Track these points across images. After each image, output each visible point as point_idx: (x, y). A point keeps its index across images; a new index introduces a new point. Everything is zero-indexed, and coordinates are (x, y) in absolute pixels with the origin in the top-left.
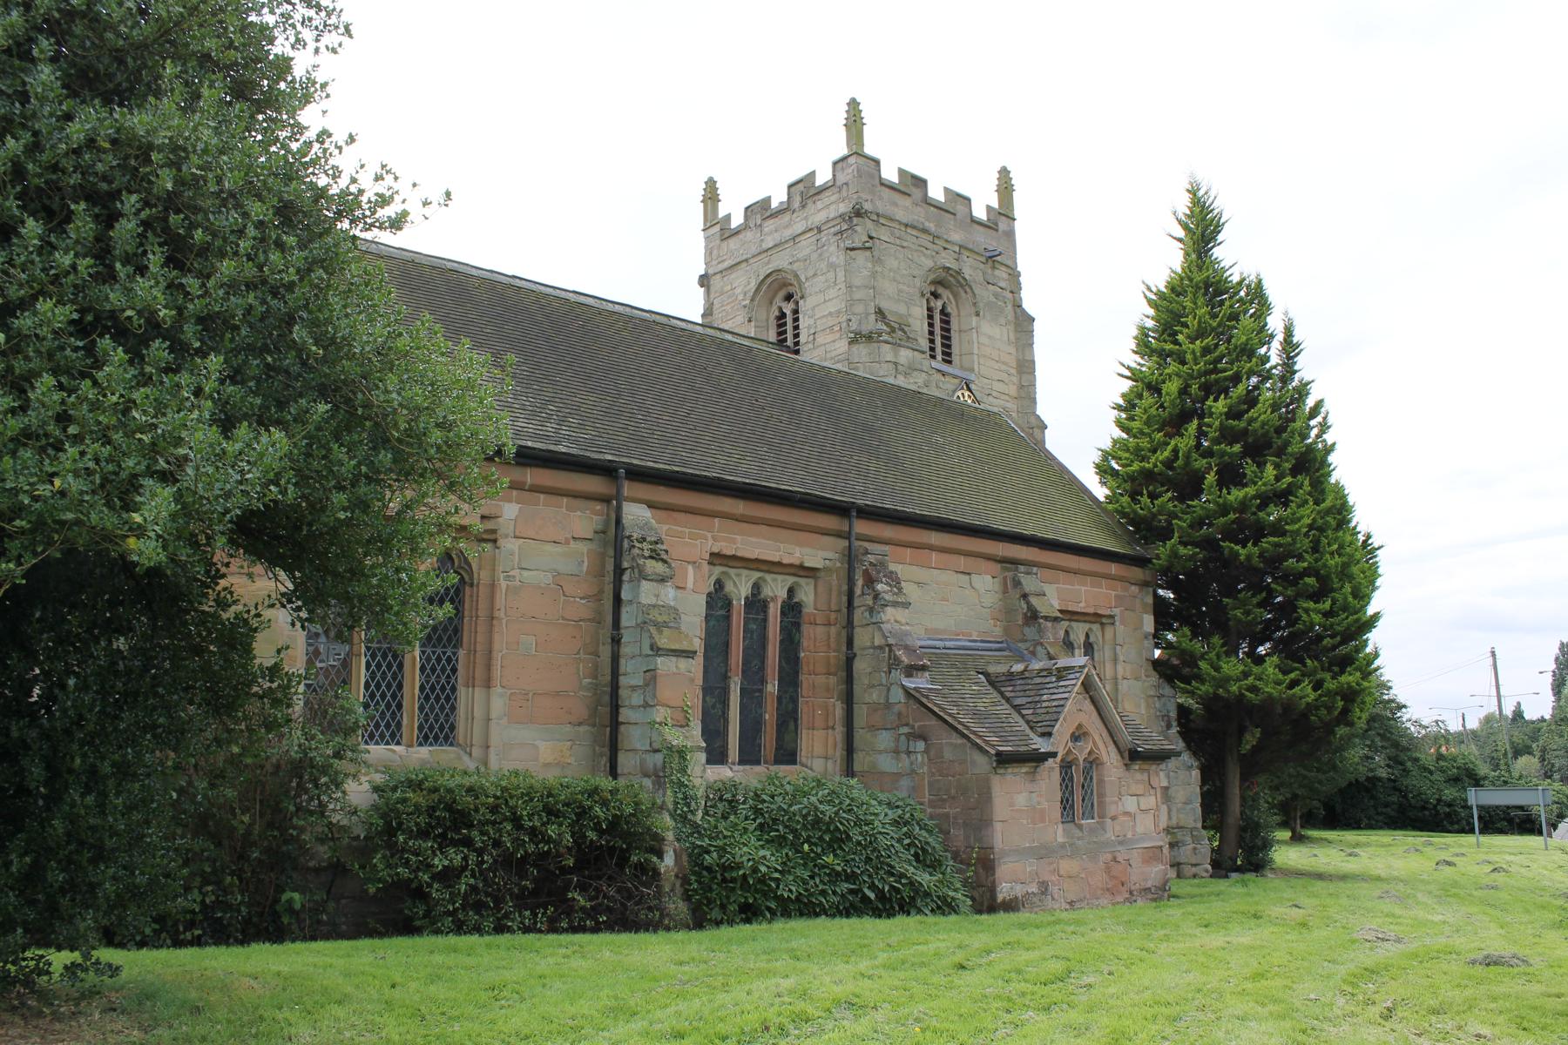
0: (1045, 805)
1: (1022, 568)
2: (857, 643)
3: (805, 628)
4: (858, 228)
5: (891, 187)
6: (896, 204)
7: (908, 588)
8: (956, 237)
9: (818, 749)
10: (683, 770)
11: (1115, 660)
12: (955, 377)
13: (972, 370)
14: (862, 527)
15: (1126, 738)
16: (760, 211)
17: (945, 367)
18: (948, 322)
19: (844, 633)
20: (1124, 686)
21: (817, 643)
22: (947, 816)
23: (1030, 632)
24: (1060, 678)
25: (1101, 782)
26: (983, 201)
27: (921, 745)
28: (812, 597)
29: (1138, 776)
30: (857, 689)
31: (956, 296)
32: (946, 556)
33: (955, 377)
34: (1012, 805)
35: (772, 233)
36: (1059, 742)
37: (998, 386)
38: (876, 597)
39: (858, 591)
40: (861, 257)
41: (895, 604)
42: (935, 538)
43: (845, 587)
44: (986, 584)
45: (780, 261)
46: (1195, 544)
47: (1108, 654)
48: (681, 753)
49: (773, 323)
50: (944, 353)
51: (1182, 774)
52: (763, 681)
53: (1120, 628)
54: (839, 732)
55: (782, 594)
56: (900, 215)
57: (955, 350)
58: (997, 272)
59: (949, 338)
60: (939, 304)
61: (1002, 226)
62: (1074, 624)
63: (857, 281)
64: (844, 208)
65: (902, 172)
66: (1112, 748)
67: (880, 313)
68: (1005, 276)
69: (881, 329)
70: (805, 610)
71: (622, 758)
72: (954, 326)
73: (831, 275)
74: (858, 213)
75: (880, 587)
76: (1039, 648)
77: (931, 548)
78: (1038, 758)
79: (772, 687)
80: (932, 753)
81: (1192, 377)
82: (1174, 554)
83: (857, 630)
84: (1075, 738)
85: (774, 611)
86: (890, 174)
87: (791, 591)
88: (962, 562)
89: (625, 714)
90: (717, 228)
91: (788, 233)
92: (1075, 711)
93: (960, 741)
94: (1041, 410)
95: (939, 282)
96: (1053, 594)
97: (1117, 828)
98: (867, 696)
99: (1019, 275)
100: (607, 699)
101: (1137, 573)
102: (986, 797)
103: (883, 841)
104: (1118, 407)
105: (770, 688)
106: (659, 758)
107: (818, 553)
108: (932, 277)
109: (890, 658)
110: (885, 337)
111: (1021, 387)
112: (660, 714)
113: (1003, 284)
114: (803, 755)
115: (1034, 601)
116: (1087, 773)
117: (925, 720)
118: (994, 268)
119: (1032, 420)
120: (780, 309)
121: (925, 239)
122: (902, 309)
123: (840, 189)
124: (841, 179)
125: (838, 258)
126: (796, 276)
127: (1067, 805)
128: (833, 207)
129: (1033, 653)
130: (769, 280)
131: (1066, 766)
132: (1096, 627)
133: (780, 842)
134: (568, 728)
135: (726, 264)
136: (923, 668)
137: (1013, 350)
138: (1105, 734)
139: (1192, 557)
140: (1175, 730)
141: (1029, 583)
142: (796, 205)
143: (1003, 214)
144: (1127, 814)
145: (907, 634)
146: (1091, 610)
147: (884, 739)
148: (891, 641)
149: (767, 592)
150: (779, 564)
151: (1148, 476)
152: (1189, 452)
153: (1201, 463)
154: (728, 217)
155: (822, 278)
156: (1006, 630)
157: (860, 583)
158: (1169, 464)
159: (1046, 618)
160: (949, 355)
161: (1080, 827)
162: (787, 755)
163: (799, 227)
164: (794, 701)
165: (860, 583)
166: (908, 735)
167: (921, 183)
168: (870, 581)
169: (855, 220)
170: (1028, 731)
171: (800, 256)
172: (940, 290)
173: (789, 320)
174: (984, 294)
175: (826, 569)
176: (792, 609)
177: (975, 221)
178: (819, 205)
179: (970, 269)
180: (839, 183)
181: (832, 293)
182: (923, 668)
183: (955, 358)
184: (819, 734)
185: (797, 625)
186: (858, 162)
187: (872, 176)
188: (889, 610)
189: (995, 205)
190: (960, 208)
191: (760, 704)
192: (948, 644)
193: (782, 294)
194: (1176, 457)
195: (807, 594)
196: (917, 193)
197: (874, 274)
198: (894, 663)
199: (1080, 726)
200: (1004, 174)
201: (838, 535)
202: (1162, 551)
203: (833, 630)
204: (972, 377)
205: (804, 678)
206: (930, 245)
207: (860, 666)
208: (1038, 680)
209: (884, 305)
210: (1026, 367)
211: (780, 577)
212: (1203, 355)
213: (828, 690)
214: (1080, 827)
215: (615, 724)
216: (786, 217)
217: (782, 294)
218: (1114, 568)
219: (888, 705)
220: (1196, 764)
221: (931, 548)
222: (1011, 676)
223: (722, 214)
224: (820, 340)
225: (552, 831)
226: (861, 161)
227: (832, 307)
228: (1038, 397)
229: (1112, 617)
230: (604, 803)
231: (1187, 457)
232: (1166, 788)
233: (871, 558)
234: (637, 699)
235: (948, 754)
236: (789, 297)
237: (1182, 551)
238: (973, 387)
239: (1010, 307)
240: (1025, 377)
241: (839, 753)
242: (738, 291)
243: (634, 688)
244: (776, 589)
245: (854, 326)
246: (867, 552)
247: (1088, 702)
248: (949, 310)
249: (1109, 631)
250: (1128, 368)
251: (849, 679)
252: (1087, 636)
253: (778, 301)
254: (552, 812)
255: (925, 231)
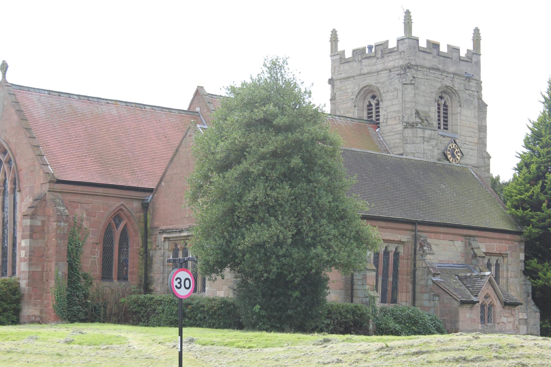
0: (475, 317)
1: (472, 238)
2: (417, 265)
3: (400, 260)
4: (409, 74)
5: (424, 51)
6: (425, 59)
7: (433, 247)
8: (452, 69)
9: (404, 300)
10: (374, 303)
11: (507, 270)
12: (449, 137)
13: (457, 133)
14: (419, 228)
15: (503, 298)
16: (358, 53)
17: (444, 133)
18: (446, 110)
19: (413, 262)
20: (511, 280)
21: (404, 265)
22: (445, 320)
23: (474, 261)
24: (481, 279)
25: (494, 312)
26: (465, 46)
27: (437, 298)
28: (402, 250)
29: (507, 311)
30: (417, 280)
31: (451, 97)
32: (445, 235)
33: (449, 137)
34: (465, 316)
35: (367, 66)
36: (480, 298)
37: (469, 139)
38: (424, 251)
39: (418, 249)
40: (410, 88)
41: (430, 254)
42: (442, 230)
43: (413, 248)
44: (459, 244)
45: (370, 81)
46: (540, 228)
47: (505, 268)
48: (374, 298)
49: (365, 108)
50: (444, 125)
51: (533, 314)
52: (387, 277)
53: (510, 258)
54: (410, 294)
55: (394, 250)
56: (428, 64)
57: (450, 123)
58: (471, 84)
59: (447, 117)
60: (443, 102)
61: (474, 59)
62: (492, 257)
63: (407, 99)
64: (401, 62)
65: (428, 42)
66: (498, 301)
67: (417, 113)
68: (474, 85)
69: (419, 121)
70: (400, 254)
71: (354, 299)
72: (449, 111)
73: (395, 93)
74: (409, 67)
75: (425, 248)
76: (477, 267)
77: (441, 233)
78: (473, 303)
79: (391, 279)
80: (441, 301)
81: (542, 163)
82: (530, 232)
83: (417, 262)
84: (487, 297)
85: (391, 255)
86: (423, 44)
87: (396, 248)
88: (451, 237)
89: (355, 287)
90: (338, 57)
91: (374, 68)
92: (486, 289)
93: (450, 297)
94: (488, 150)
95: (444, 92)
96: (482, 247)
97: (499, 327)
98: (420, 282)
99: (481, 82)
100: (349, 282)
101: (518, 237)
102: (457, 314)
103: (428, 324)
104: (515, 169)
105: (390, 279)
106: (367, 299)
107: (405, 237)
108: (440, 91)
109: (428, 270)
110: (419, 126)
111: (480, 138)
112: (367, 287)
113: (473, 89)
114: (399, 301)
115: (476, 251)
116: (489, 309)
117: (438, 290)
118: (469, 81)
119: (484, 154)
120: (370, 102)
121: (438, 74)
122: (426, 109)
123: (401, 53)
124: (401, 48)
125: (399, 86)
126: (379, 90)
127: (482, 318)
128: (397, 61)
129: (475, 269)
130: (365, 89)
131: (483, 306)
132: (500, 258)
133: (400, 323)
134: (338, 291)
135: (343, 76)
136: (438, 274)
137: (476, 121)
138: (496, 297)
139: (537, 233)
140: (530, 297)
141: (474, 244)
142: (379, 55)
143: (475, 52)
144: (503, 323)
145: (433, 263)
146: (498, 252)
147: (426, 296)
148: (428, 265)
149: (389, 249)
150: (394, 241)
151: (523, 200)
152: (538, 194)
153: (542, 197)
154: (343, 52)
155: (391, 94)
156: (466, 260)
157: (418, 246)
158: (531, 197)
159: (479, 257)
160: (447, 125)
161: (487, 325)
162: (394, 301)
163: (380, 67)
164: (396, 283)
165: (418, 246)
166: (434, 295)
167: (436, 46)
168: (422, 246)
169: (407, 70)
170: (471, 295)
171: (381, 81)
172: (444, 95)
173: (374, 107)
174: (464, 95)
175: (408, 241)
176: (396, 254)
177: (460, 59)
178: (390, 58)
179: (458, 85)
180: (400, 50)
181: (396, 102)
182: (438, 274)
183: (449, 127)
184: (404, 294)
185: (398, 259)
186: (409, 40)
187: (415, 48)
188: (428, 256)
189: (471, 48)
190: (455, 55)
191: (386, 285)
192: (446, 265)
193: (370, 95)
194: (533, 195)
195: (401, 250)
196: (435, 52)
197: (415, 94)
198: (429, 273)
199: (487, 294)
200: (477, 31)
201: (412, 231)
202: (527, 230)
203: (409, 261)
204: (457, 136)
205: (400, 277)
206: (440, 76)
207: (418, 273)
208: (475, 279)
209: (420, 108)
210: (482, 129)
211: (393, 245)
212: (547, 154)
213: (407, 280)
214: (487, 325)
215: (352, 289)
216: (374, 60)
217: (371, 99)
218: (508, 236)
219: (427, 286)
220: (538, 310)
221: (441, 233)
222: (466, 277)
223: (340, 49)
224: (390, 122)
225: (348, 316)
226: (411, 41)
227: (396, 108)
228: (488, 143)
229: (507, 254)
230: (359, 310)
231: (537, 195)
232: (527, 319)
233: (422, 239)
234: (360, 283)
235: (446, 301)
236: (374, 97)
237: (534, 231)
238: (457, 141)
239: (476, 100)
240: (482, 134)
241: (410, 300)
242: (349, 91)
243: (359, 280)
244: (392, 248)
245: (406, 119)
246: (421, 237)
247: (490, 287)
248: (447, 104)
249: (506, 259)
250: (520, 154)
251: (414, 277)
252: (497, 261)
253: (369, 98)
254: (347, 311)
255: (438, 69)
